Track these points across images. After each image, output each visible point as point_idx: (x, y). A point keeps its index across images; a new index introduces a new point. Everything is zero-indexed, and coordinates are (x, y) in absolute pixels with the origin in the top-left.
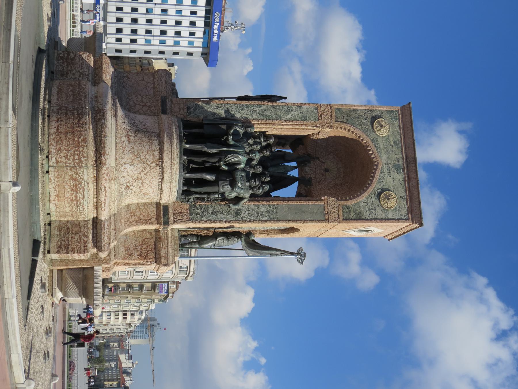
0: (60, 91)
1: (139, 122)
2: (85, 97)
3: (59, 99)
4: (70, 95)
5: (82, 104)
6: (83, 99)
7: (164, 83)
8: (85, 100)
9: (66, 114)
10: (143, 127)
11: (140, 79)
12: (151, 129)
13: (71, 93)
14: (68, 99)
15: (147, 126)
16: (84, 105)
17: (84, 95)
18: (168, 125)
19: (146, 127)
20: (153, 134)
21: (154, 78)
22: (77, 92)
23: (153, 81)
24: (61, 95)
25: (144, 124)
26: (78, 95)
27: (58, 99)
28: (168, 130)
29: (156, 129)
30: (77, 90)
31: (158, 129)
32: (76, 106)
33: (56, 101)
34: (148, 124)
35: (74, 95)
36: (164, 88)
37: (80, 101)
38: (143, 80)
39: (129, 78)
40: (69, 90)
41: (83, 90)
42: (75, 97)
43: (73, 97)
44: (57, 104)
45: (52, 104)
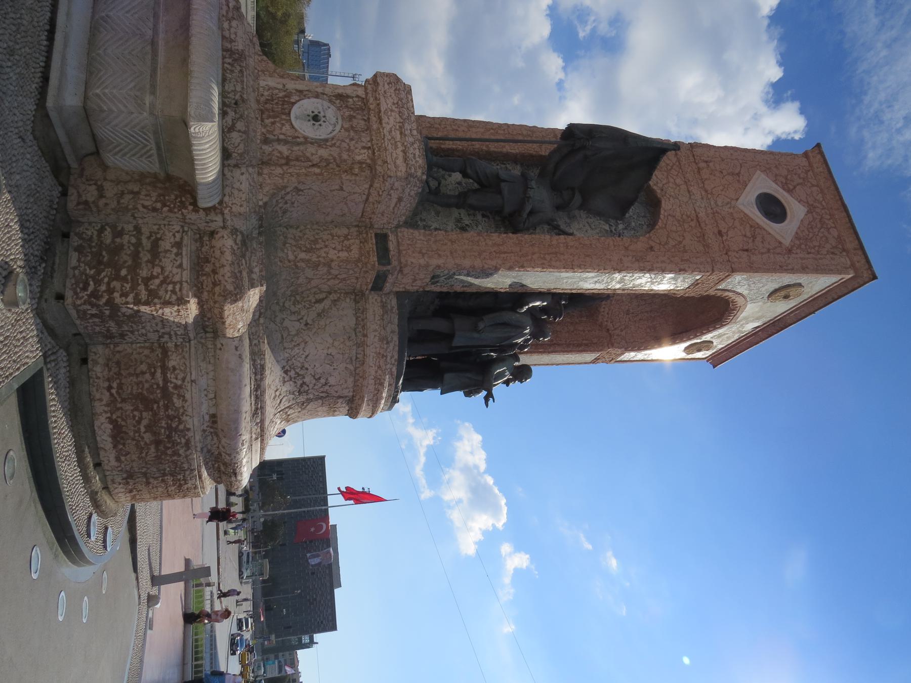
0: (118, 434)
1: (314, 376)
2: (187, 445)
3: (123, 458)
4: (146, 443)
5: (182, 463)
6: (181, 452)
7: (394, 200)
8: (188, 453)
9: (148, 483)
10: (322, 389)
11: (333, 188)
12: (337, 392)
13: (148, 437)
14: (144, 455)
15: (330, 386)
16: (186, 466)
17: (183, 441)
18: (375, 384)
19: (327, 388)
20: (340, 401)
21: (371, 186)
22: (163, 431)
23: (367, 191)
24: (124, 445)
25: (323, 381)
26: (169, 442)
27: (118, 459)
28: (372, 395)
29: (347, 390)
30: (163, 424)
31: (352, 390)
32: (168, 469)
33: (113, 463)
34: (332, 381)
35: (158, 443)
36: (391, 208)
37: (175, 458)
38: (341, 189)
39: (302, 191)
40: (143, 429)
41: (180, 422)
42: (161, 448)
43: (157, 450)
44: (120, 469)
45: (108, 471)
